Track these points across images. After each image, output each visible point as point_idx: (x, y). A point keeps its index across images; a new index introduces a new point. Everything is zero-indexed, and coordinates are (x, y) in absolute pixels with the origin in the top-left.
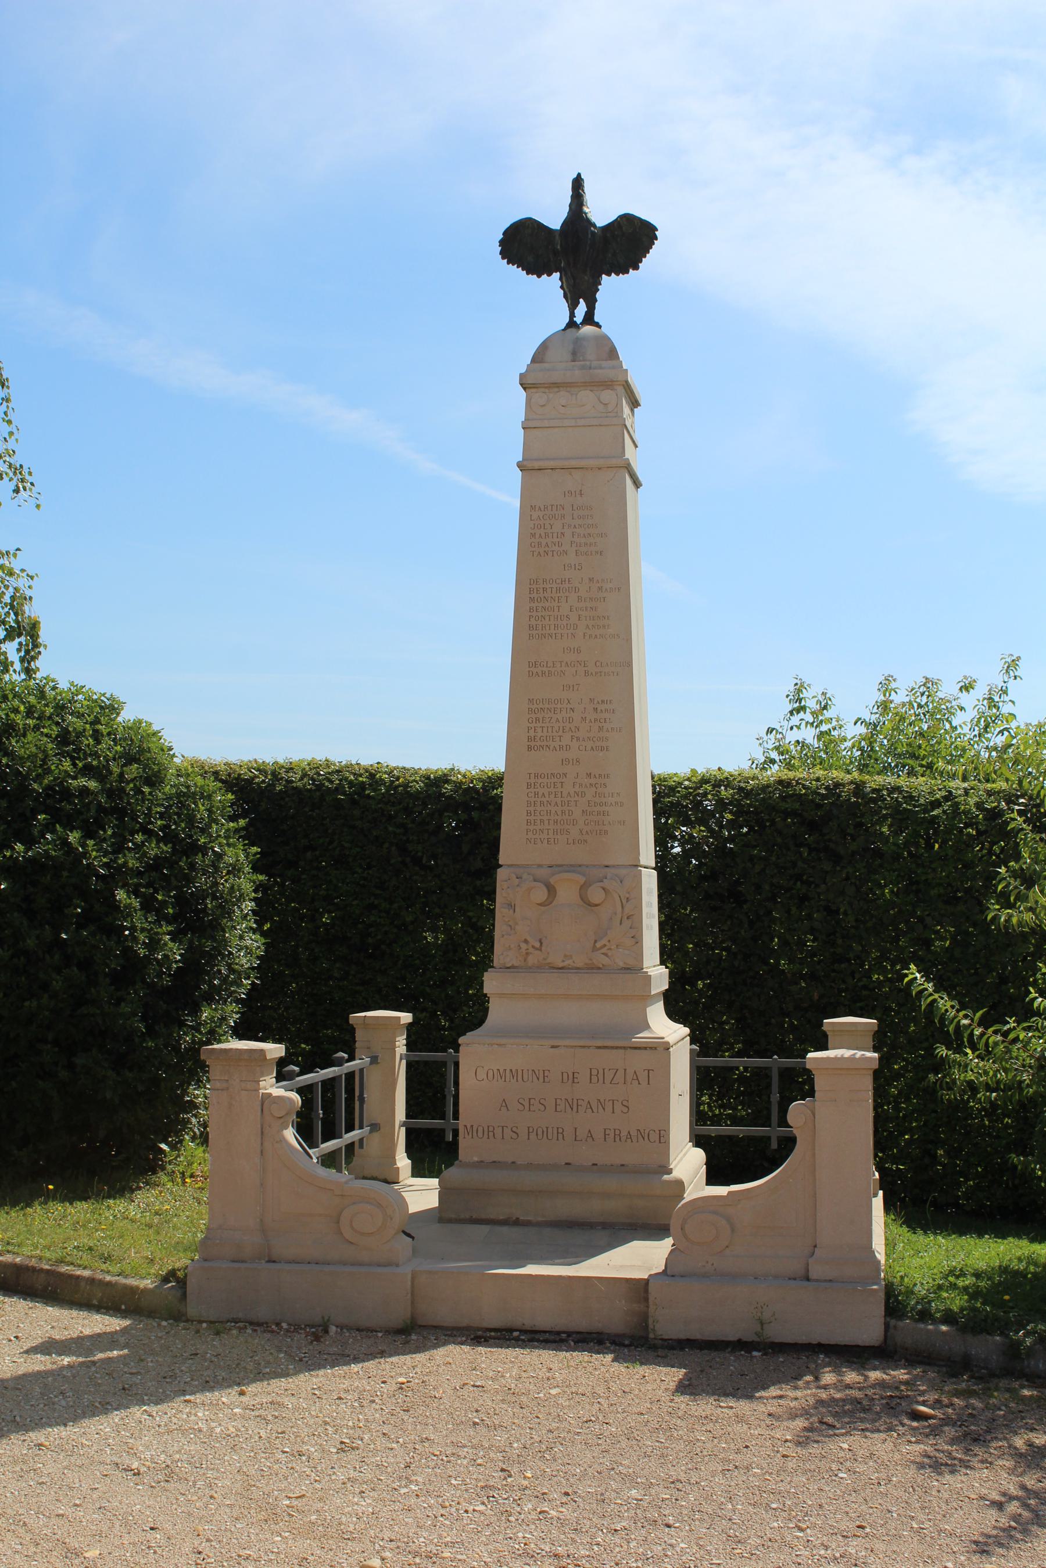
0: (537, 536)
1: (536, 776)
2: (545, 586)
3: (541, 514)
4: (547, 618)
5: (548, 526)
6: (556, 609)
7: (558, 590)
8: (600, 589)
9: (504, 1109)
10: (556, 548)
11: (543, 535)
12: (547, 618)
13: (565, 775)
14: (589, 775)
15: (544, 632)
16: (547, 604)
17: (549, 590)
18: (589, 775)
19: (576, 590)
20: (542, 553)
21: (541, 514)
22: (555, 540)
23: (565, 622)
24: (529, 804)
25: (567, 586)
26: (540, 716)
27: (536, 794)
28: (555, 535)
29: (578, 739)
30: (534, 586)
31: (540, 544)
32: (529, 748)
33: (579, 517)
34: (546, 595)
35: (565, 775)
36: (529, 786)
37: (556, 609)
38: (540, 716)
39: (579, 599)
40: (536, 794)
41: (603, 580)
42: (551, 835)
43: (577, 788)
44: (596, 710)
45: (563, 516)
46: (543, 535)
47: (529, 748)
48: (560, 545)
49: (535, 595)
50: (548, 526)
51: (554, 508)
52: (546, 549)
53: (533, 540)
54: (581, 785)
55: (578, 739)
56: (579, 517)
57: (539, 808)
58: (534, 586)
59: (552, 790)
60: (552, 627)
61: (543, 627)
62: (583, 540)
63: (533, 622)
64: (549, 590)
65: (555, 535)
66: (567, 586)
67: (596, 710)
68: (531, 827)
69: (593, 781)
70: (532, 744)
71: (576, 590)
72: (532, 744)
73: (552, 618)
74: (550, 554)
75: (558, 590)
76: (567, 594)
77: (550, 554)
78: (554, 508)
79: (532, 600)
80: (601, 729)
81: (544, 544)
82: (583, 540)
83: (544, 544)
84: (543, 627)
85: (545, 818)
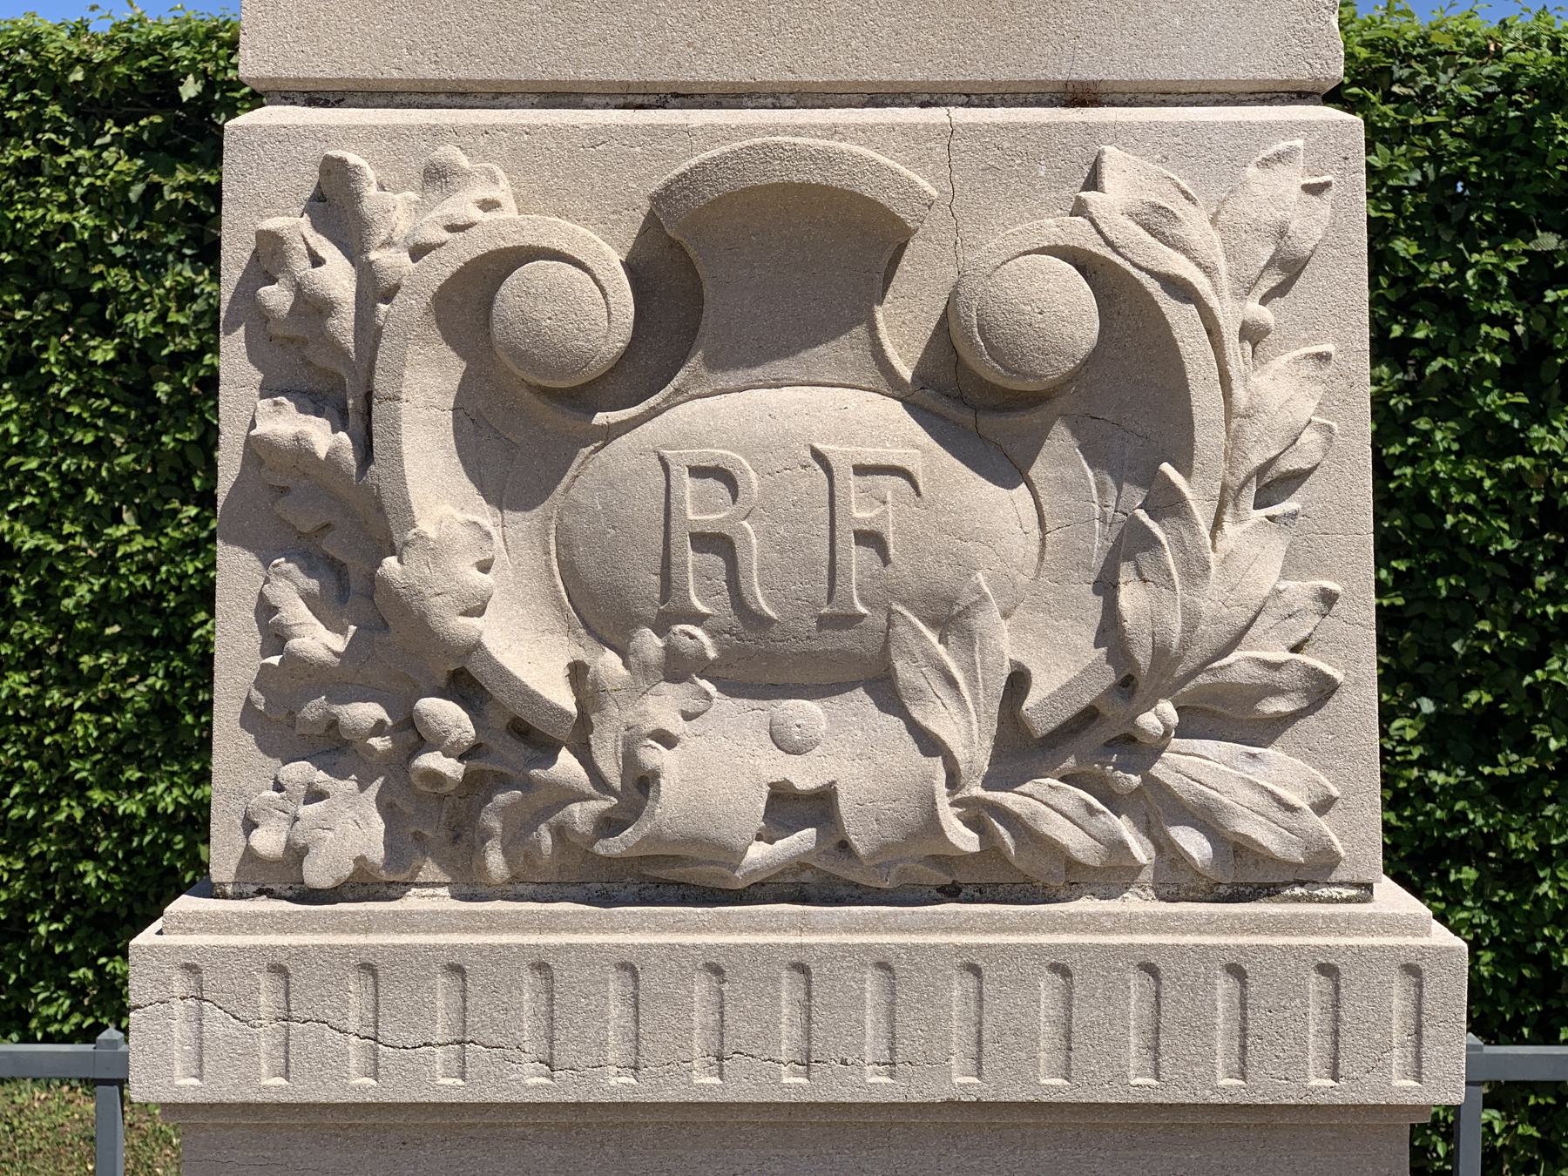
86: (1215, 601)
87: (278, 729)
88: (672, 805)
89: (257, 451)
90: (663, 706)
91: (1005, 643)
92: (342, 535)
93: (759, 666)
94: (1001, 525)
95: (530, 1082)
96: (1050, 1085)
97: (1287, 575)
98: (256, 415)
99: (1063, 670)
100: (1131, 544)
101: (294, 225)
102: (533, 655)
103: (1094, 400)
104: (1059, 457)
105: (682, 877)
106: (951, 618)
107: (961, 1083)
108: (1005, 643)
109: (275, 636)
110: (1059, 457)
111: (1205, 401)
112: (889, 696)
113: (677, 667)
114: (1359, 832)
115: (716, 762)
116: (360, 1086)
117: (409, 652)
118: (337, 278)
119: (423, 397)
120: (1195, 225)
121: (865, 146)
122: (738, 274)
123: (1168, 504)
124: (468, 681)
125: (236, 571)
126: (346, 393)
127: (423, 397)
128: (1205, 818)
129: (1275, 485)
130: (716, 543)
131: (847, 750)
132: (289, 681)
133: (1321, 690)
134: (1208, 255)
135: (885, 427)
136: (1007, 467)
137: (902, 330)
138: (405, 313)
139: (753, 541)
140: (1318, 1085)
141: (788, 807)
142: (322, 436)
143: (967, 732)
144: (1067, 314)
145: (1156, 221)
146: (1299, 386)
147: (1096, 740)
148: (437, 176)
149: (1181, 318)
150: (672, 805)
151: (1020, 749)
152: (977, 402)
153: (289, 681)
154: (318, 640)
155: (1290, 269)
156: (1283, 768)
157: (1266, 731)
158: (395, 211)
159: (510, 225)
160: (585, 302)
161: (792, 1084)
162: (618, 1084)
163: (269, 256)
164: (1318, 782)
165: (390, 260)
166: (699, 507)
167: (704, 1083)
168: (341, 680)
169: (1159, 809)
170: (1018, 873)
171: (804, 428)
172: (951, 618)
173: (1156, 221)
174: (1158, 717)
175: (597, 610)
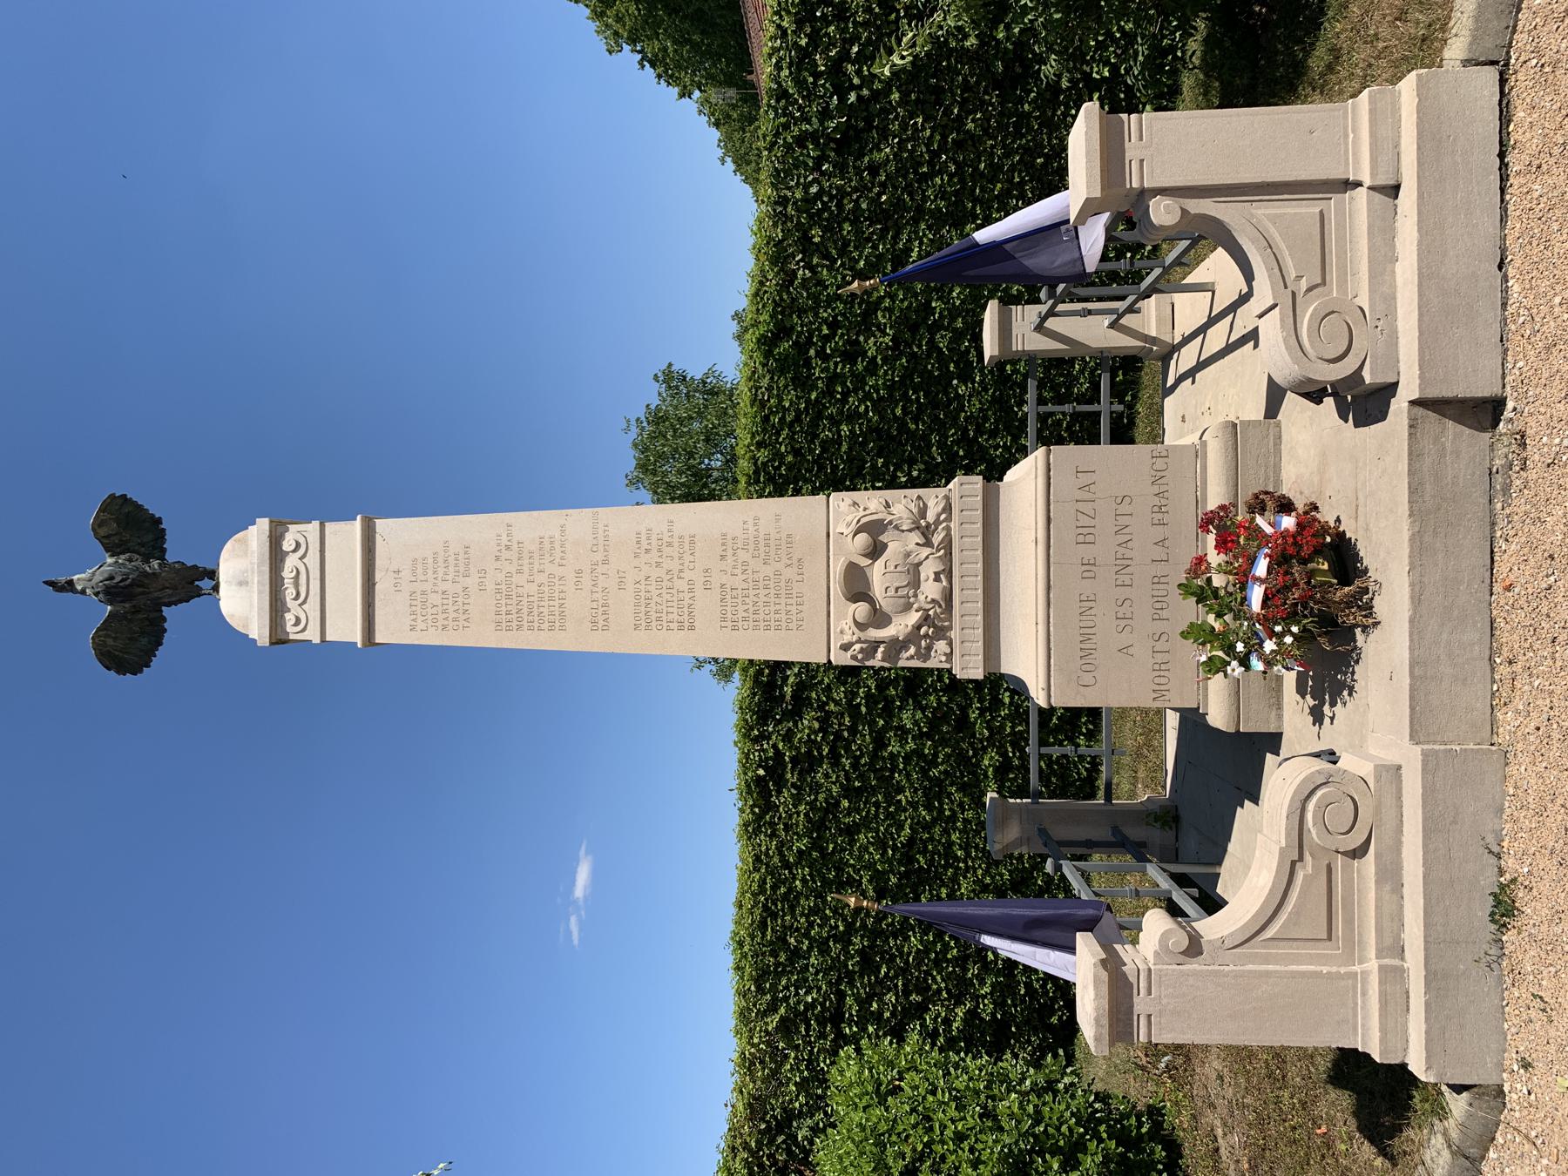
1: (724, 619)
5: (434, 610)
7: (508, 597)
8: (508, 548)
9: (1131, 651)
10: (460, 600)
13: (722, 585)
14: (723, 557)
16: (525, 610)
18: (723, 557)
19: (509, 575)
24: (756, 628)
25: (503, 587)
26: (654, 616)
27: (745, 619)
29: (681, 571)
31: (455, 620)
32: (692, 628)
33: (425, 573)
35: (722, 585)
36: (735, 628)
38: (654, 616)
39: (519, 572)
40: (745, 619)
42: (793, 601)
43: (739, 571)
44: (647, 551)
45: (424, 593)
47: (692, 628)
48: (456, 595)
50: (434, 610)
54: (734, 567)
55: (681, 571)
56: (425, 573)
57: (761, 616)
59: (739, 601)
61: (551, 614)
63: (545, 626)
66: (503, 587)
67: (647, 551)
68: (784, 625)
69: (730, 552)
70: (686, 624)
71: (509, 575)
72: (686, 624)
75: (508, 597)
79: (519, 628)
80: (670, 545)
84: (551, 614)
85: (773, 608)
86: (905, 514)
87: (926, 657)
88: (937, 597)
89: (883, 660)
90: (921, 598)
91: (912, 546)
92: (896, 646)
93: (915, 583)
94: (895, 546)
95: (980, 618)
96: (980, 539)
97: (902, 503)
98: (877, 661)
99: (916, 537)
100: (896, 527)
101: (849, 653)
102: (914, 617)
103: (875, 533)
104: (883, 538)
105: (948, 596)
106: (908, 555)
107: (980, 552)
108: (912, 546)
109: (912, 657)
110: (883, 538)
111: (875, 517)
112: (920, 564)
113: (916, 596)
114: (942, 492)
115: (930, 590)
116: (981, 644)
117: (913, 636)
118: (857, 647)
119: (874, 634)
120: (849, 518)
121: (838, 568)
122: (857, 586)
123: (890, 522)
124: (919, 628)
125: (901, 664)
126: (876, 644)
127: (874, 634)
128: (939, 515)
129: (888, 505)
130: (897, 590)
131: (928, 570)
132: (918, 655)
133: (919, 498)
134: (853, 517)
135: (880, 563)
136: (885, 546)
137: (864, 562)
138: (863, 636)
139: (897, 584)
140: (980, 498)
141: (937, 579)
142: (881, 649)
143: (926, 551)
144: (863, 538)
145: (848, 525)
146: (872, 502)
147: (927, 533)
148: (842, 632)
149: (864, 520)
150: (937, 597)
151: (928, 544)
152: (876, 551)
153: (918, 655)
154: (912, 650)
155: (855, 504)
156: (931, 504)
157: (925, 505)
158: (847, 638)
159: (850, 621)
160: (862, 609)
161: (980, 578)
162: (980, 605)
163: (854, 658)
164: (933, 498)
165: (855, 638)
166: (891, 592)
167: (980, 591)
168: (919, 647)
169: (937, 522)
170: (948, 544)
171: (880, 577)
172: (908, 555)
173: (848, 525)
174: (923, 523)
175: (907, 607)
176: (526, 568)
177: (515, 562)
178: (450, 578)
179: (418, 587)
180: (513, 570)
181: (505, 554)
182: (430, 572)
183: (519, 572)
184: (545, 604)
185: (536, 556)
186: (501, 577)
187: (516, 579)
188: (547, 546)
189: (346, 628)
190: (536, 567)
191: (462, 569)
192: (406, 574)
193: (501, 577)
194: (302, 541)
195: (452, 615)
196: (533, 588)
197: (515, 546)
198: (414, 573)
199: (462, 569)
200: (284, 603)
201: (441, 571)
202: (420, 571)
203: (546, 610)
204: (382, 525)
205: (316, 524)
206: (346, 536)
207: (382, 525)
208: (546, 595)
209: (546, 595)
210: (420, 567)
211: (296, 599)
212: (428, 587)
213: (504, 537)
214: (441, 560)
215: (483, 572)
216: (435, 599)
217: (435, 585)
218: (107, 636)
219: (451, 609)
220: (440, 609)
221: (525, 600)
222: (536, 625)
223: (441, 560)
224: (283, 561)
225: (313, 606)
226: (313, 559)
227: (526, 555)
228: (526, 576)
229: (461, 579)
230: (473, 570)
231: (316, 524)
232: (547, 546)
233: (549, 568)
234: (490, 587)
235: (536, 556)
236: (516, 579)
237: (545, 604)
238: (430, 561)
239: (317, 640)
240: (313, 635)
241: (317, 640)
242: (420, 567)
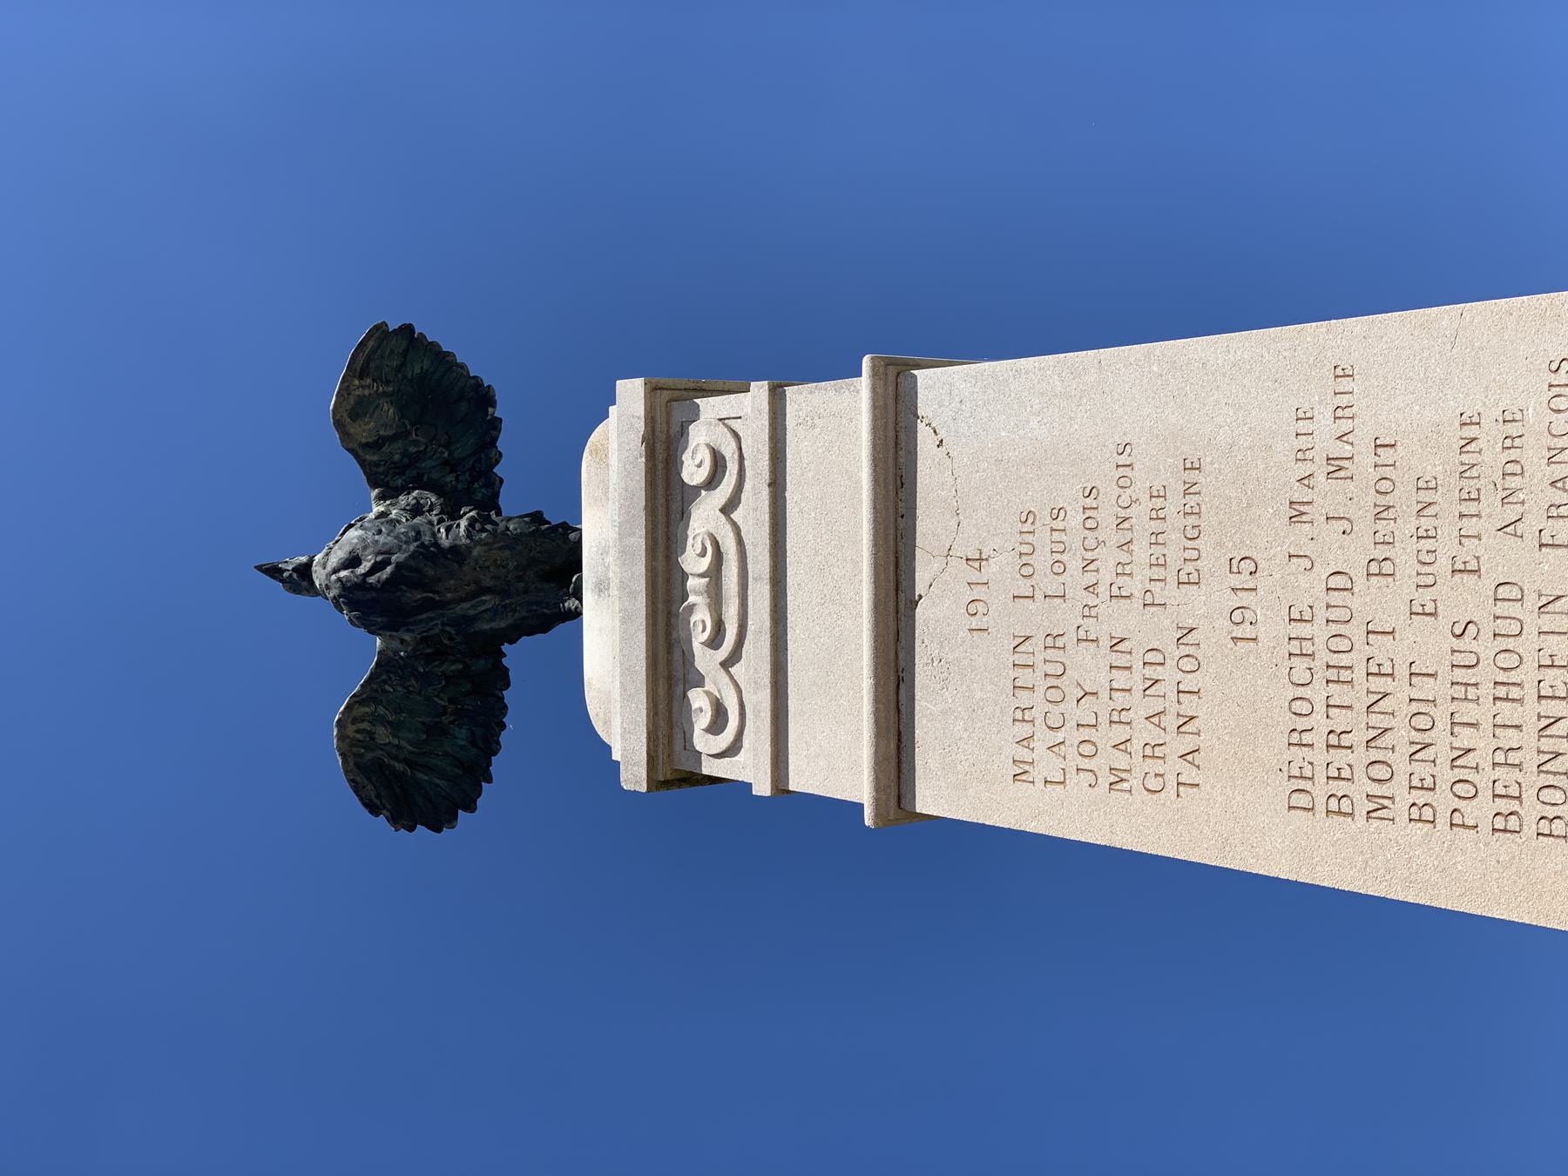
0: (1122, 761)
2: (1318, 738)
3: (1044, 738)
4: (1466, 738)
5: (1084, 713)
6: (1426, 688)
7: (1338, 675)
8: (1337, 467)
11: (1120, 733)
12: (1466, 738)
15: (1530, 759)
16: (1402, 736)
17: (1340, 720)
19: (1339, 583)
20: (1188, 743)
21: (1044, 738)
22: (1136, 681)
23: (1486, 648)
25: (1319, 631)
28: (1121, 679)
30: (1320, 789)
31: (1153, 752)
34: (1358, 737)
37: (1426, 688)
39: (1379, 569)
41: (1302, 456)
45: (1054, 640)
46: (1120, 733)
49: (1361, 788)
50: (1084, 713)
51: (1026, 677)
52: (1170, 721)
53: (1135, 783)
58: (1320, 789)
60: (1508, 712)
61: (1506, 758)
62: (1141, 552)
63: (1481, 810)
64: (1340, 720)
65: (1121, 679)
66: (1318, 631)
71: (1339, 583)
73: (1468, 712)
74: (1189, 705)
75: (1338, 675)
76: (1356, 631)
77: (1189, 705)
78: (1026, 677)
79: (1378, 809)
81: (1149, 733)
82: (1141, 552)
83: (1149, 733)
84: (1506, 758)
176: (1404, 555)
177: (1364, 525)
178: (1134, 586)
179: (1036, 618)
180: (1355, 554)
181: (1327, 495)
182: (1074, 565)
183: (1379, 569)
184: (1481, 712)
185: (1446, 502)
186: (1310, 589)
187: (1382, 603)
188: (1491, 458)
189: (834, 761)
190: (1446, 547)
191: (1174, 555)
192: (1001, 568)
193: (1310, 589)
194: (729, 451)
195: (1145, 734)
196: (1427, 644)
197: (1365, 459)
198: (1026, 569)
199: (1174, 555)
200: (688, 657)
201: (1108, 559)
202: (1041, 561)
203: (1481, 742)
204: (936, 387)
205: (759, 391)
206: (834, 420)
207: (936, 387)
208: (1485, 674)
209: (1485, 674)
210: (1042, 538)
211: (715, 642)
212: (1066, 617)
213: (1324, 417)
214: (1106, 516)
215: (1244, 564)
216: (1089, 667)
217: (1089, 611)
218: (375, 719)
219: (1141, 708)
220: (1103, 705)
221: (1400, 691)
222: (1443, 801)
223: (1106, 516)
224: (684, 515)
225: (755, 666)
226: (754, 514)
227: (1404, 497)
228: (1404, 587)
229: (1168, 592)
230: (1212, 560)
231: (759, 391)
232: (1491, 458)
233: (1504, 558)
234: (1272, 629)
235: (1446, 502)
236: (1382, 603)
237: (1481, 712)
238: (1075, 519)
239: (762, 788)
240: (751, 769)
241: (762, 788)
242: (1042, 538)
